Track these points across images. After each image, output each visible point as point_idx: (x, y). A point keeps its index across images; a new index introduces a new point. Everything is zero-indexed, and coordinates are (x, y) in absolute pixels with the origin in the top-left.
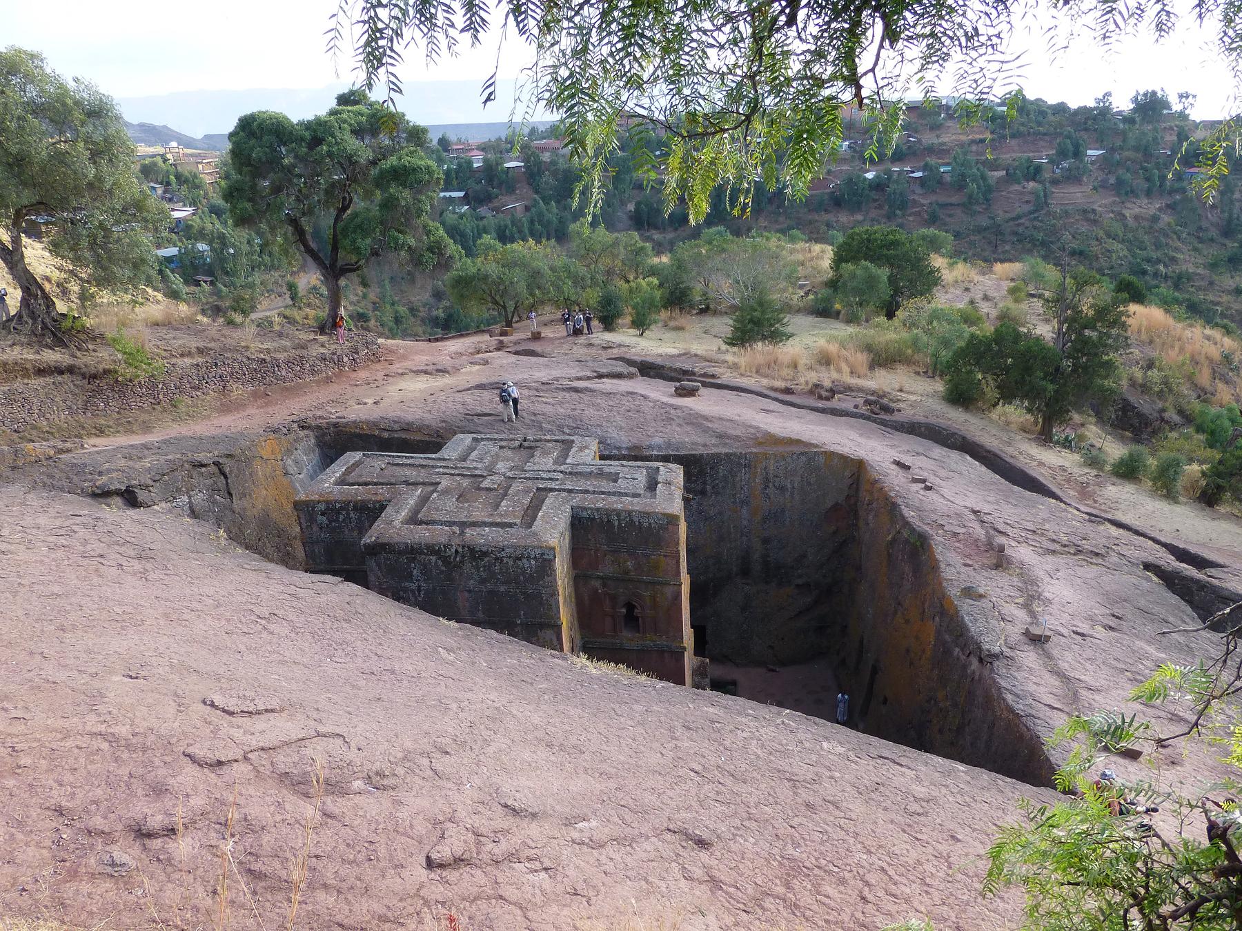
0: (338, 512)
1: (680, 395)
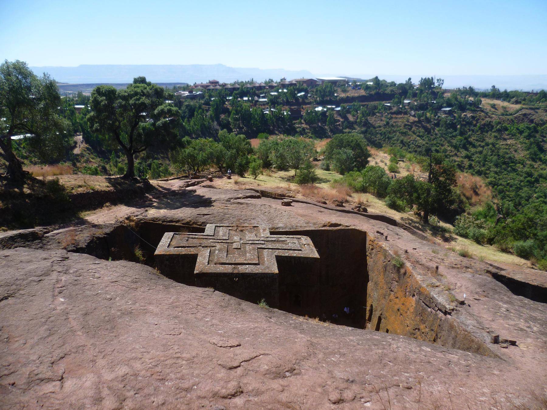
1: (284, 205)
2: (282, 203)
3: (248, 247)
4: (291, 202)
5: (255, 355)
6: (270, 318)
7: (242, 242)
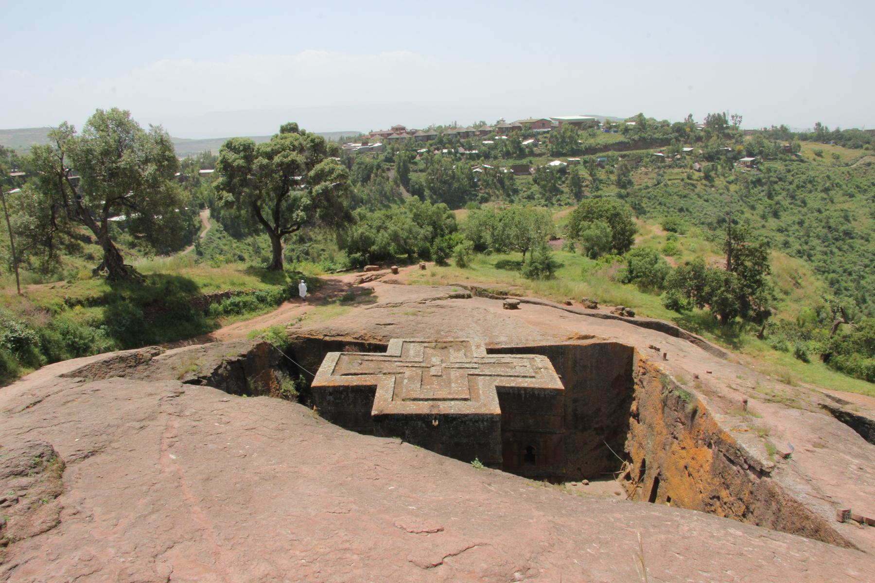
0: (341, 393)
1: (507, 308)
2: (505, 304)
3: (454, 374)
4: (518, 303)
5: (467, 546)
6: (490, 485)
7: (444, 365)
